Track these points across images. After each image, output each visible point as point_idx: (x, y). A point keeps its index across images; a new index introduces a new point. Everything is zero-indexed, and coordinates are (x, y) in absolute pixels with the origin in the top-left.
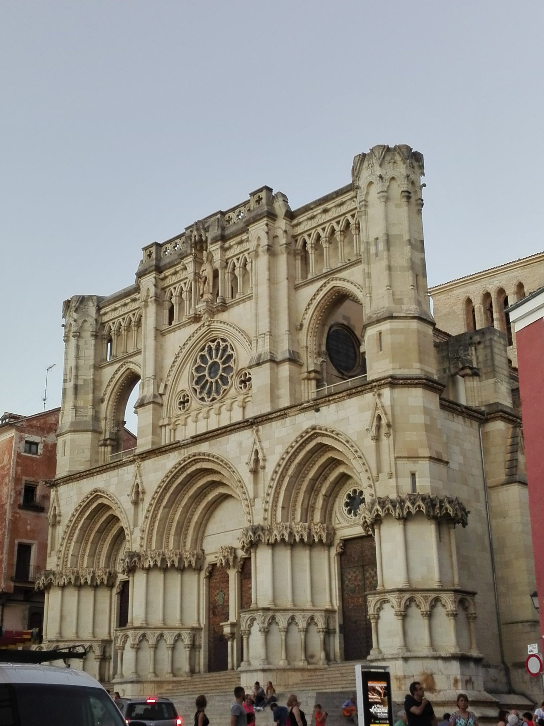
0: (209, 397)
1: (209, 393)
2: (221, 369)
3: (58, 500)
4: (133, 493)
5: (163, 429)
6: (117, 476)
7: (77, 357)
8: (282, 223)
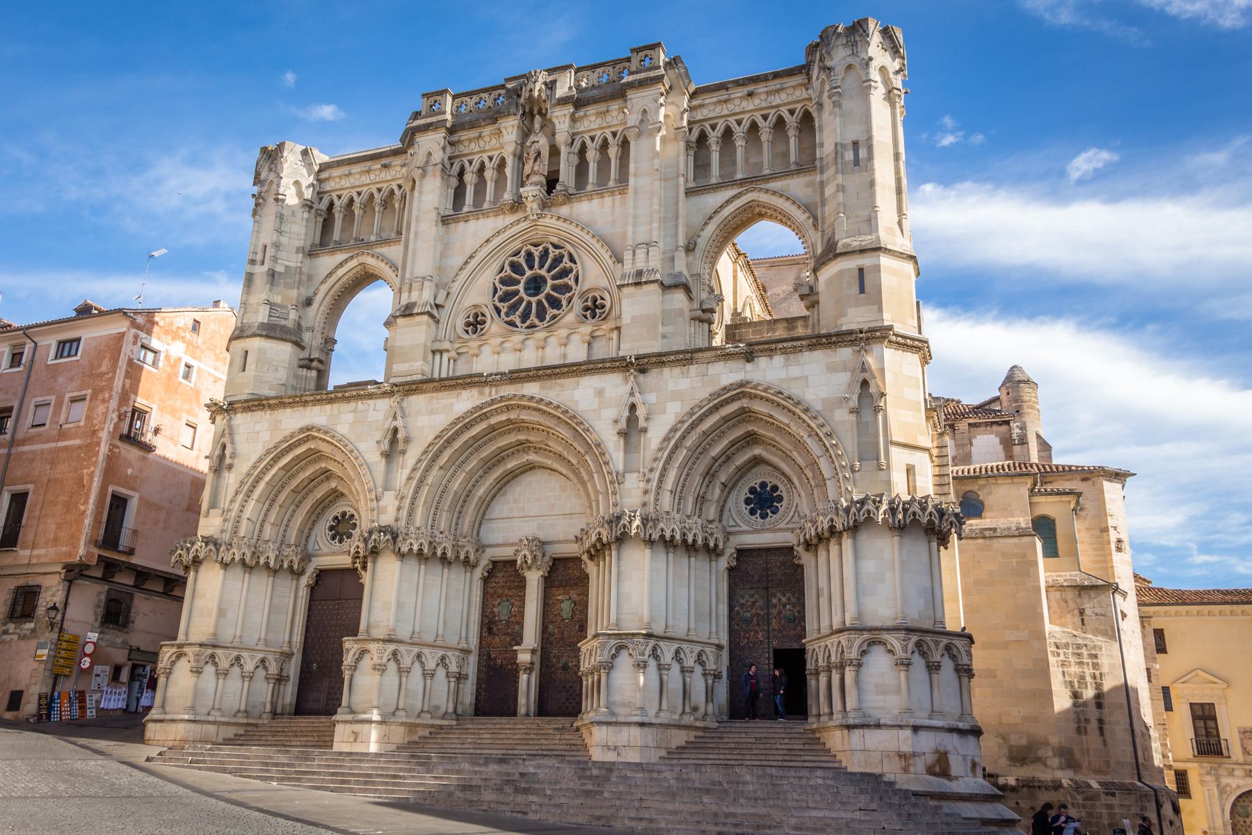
0: (523, 322)
1: (525, 316)
3: (231, 434)
4: (386, 442)
5: (438, 357)
6: (354, 411)
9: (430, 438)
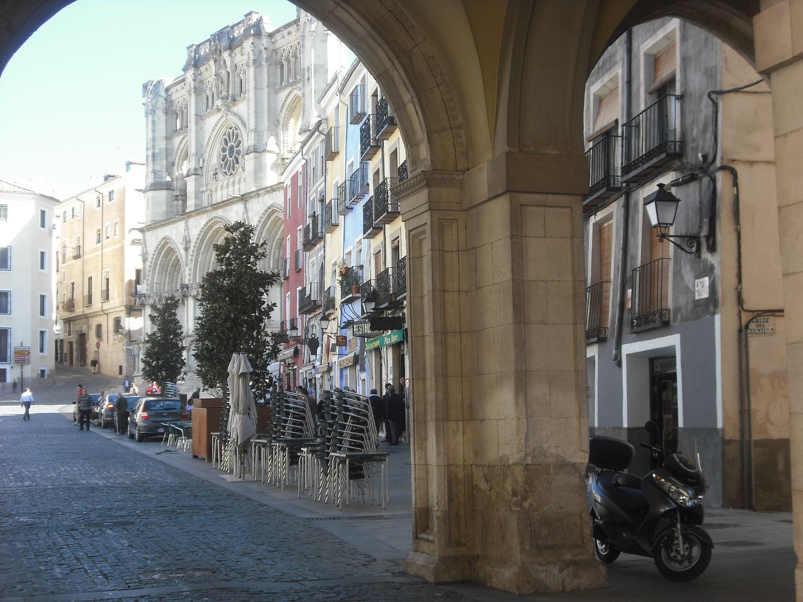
1: (229, 170)
7: (154, 131)
8: (265, 41)
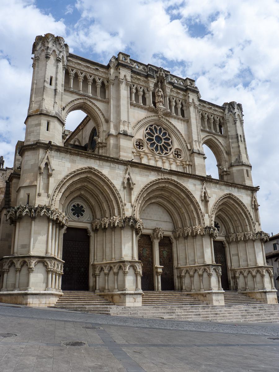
1: (157, 149)
2: (163, 141)
6: (110, 166)
9: (142, 186)
